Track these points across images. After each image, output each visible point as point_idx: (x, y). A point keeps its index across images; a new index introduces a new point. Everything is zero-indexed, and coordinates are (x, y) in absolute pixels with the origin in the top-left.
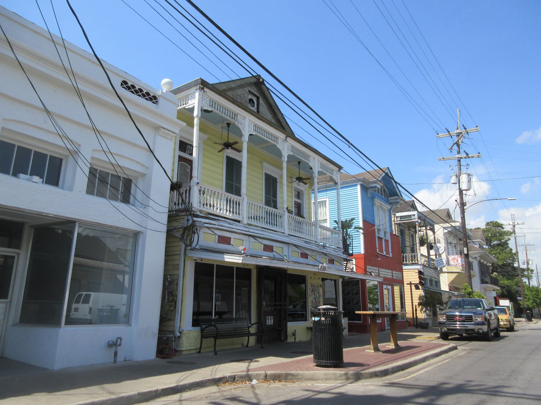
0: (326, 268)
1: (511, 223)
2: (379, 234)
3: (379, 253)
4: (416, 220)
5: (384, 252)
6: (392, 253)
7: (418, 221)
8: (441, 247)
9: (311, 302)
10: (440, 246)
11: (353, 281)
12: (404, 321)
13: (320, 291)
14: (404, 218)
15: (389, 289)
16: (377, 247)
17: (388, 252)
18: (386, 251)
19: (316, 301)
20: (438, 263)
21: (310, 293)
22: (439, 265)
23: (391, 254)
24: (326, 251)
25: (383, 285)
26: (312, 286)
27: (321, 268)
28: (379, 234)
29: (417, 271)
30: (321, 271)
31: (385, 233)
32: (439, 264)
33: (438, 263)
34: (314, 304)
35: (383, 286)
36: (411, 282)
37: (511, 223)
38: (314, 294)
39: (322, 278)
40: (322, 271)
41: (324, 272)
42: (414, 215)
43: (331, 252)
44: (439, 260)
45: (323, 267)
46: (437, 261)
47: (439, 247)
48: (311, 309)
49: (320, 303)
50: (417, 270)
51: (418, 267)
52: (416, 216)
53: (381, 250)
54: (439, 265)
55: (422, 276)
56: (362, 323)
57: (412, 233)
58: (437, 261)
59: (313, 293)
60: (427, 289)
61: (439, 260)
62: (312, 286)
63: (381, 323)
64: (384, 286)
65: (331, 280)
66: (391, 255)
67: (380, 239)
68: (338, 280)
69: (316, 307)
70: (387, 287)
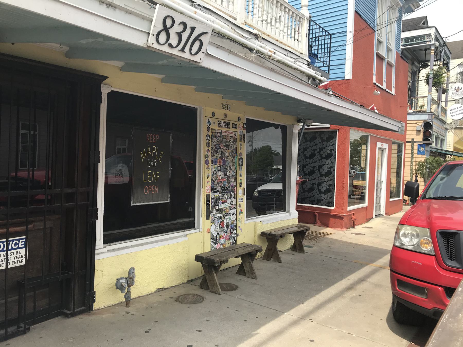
0: (205, 39)
2: (378, 49)
3: (377, 84)
4: (433, 42)
5: (385, 84)
6: (396, 88)
7: (434, 45)
8: (461, 88)
9: (210, 179)
10: (461, 87)
11: (323, 132)
12: (401, 199)
13: (239, 151)
14: (411, 40)
15: (385, 149)
16: (375, 73)
17: (389, 86)
18: (387, 82)
19: (225, 174)
20: (452, 113)
21: (206, 157)
22: (455, 115)
23: (393, 90)
24: (261, 47)
25: (377, 142)
26: (216, 137)
27: (166, 29)
28: (378, 49)
29: (421, 123)
30: (166, 49)
31: (389, 50)
33: (452, 113)
34: (218, 183)
35: (376, 142)
38: (222, 157)
39: (247, 119)
40: (175, 52)
41: (186, 55)
42: (429, 35)
43: (274, 53)
44: (455, 109)
45: (177, 28)
46: (451, 110)
47: (459, 88)
48: (208, 196)
49: (239, 179)
50: (423, 121)
52: (433, 36)
53: (380, 79)
54: (455, 115)
55: (430, 131)
56: (334, 210)
57: (415, 69)
58: (451, 110)
59: (218, 155)
60: (434, 150)
61: (455, 109)
62: (216, 137)
63: (367, 207)
64: (379, 145)
65: (276, 126)
66: (393, 92)
67: (380, 58)
68: (292, 127)
69: (224, 190)
70: (382, 145)
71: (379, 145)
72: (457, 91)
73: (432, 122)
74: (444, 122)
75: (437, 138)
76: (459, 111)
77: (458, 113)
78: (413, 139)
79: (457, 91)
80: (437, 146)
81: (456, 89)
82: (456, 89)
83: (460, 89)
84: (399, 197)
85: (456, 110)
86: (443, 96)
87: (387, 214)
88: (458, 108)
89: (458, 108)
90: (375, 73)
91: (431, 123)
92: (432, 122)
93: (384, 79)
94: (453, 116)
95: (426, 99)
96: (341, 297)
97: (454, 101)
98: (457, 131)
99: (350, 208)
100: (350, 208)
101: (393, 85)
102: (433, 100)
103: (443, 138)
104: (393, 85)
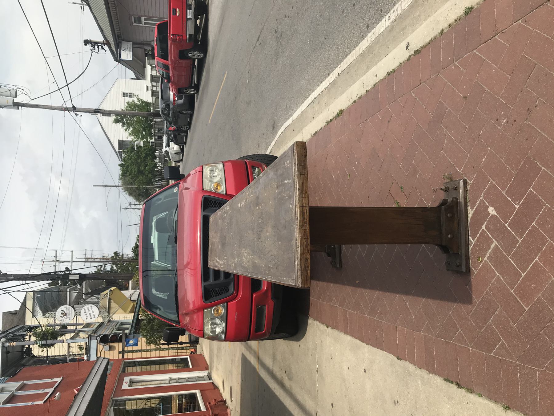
1: (54, 264)
3: (46, 399)
6: (53, 377)
8: (63, 311)
12: (190, 357)
15: (130, 379)
16: (30, 404)
17: (50, 385)
22: (94, 315)
23: (55, 380)
29: (101, 346)
32: (92, 314)
35: (122, 390)
36: (120, 352)
37: (54, 264)
46: (87, 319)
47: (62, 313)
50: (99, 345)
51: (94, 343)
54: (94, 315)
55: (110, 336)
57: (32, 361)
58: (87, 319)
60: (133, 330)
61: (86, 314)
63: (201, 391)
64: (125, 387)
66: (59, 380)
70: (126, 383)
71: (125, 387)
72: (66, 315)
73: (100, 335)
74: (101, 324)
75: (119, 329)
76: (89, 310)
77: (91, 312)
78: (120, 352)
79: (66, 315)
80: (129, 328)
81: (62, 315)
82: (62, 315)
83: (63, 312)
84: (187, 358)
85: (88, 313)
86: (69, 328)
87: (207, 369)
88: (85, 312)
89: (85, 312)
90: (30, 404)
91: (101, 336)
92: (100, 335)
93: (40, 391)
94: (94, 316)
95: (71, 345)
96: (291, 391)
97: (77, 317)
98: (112, 311)
99: (203, 408)
100: (203, 408)
101: (50, 380)
102: (73, 338)
103: (119, 324)
104: (50, 380)
